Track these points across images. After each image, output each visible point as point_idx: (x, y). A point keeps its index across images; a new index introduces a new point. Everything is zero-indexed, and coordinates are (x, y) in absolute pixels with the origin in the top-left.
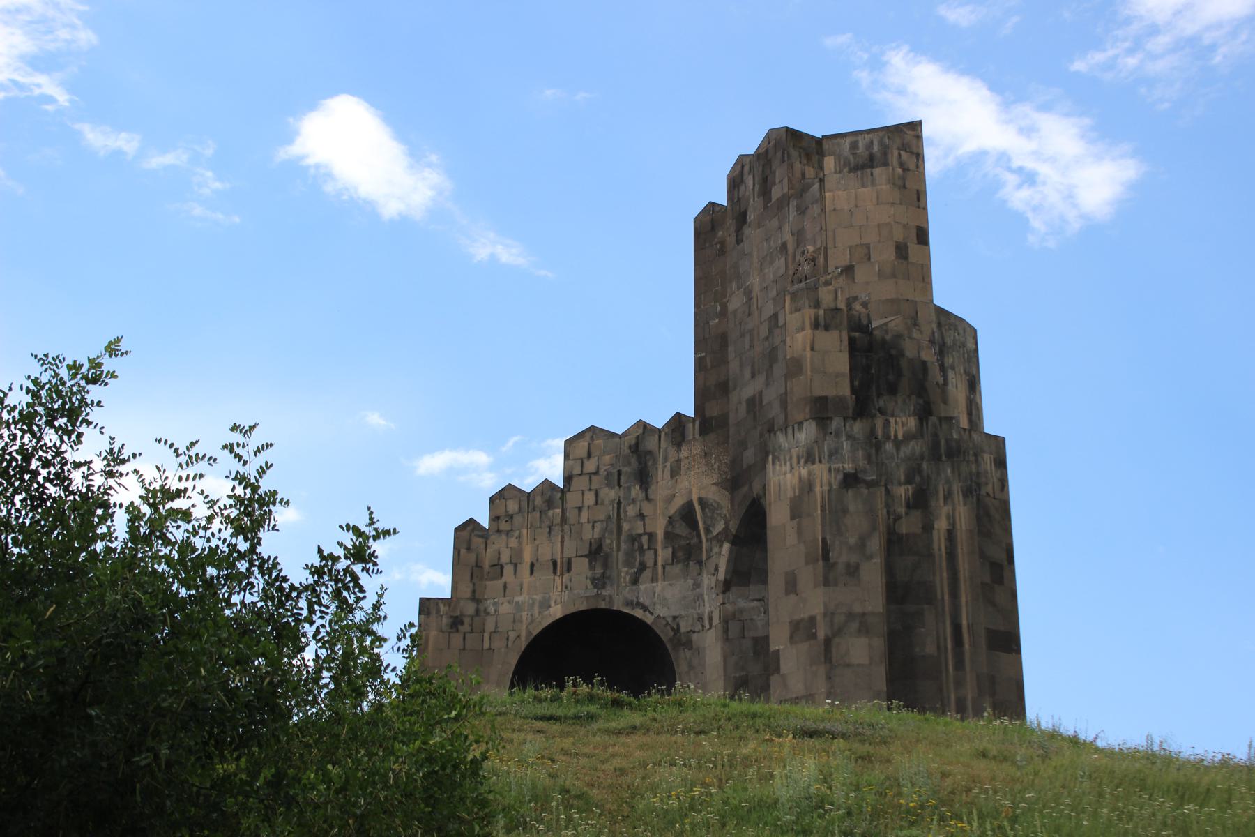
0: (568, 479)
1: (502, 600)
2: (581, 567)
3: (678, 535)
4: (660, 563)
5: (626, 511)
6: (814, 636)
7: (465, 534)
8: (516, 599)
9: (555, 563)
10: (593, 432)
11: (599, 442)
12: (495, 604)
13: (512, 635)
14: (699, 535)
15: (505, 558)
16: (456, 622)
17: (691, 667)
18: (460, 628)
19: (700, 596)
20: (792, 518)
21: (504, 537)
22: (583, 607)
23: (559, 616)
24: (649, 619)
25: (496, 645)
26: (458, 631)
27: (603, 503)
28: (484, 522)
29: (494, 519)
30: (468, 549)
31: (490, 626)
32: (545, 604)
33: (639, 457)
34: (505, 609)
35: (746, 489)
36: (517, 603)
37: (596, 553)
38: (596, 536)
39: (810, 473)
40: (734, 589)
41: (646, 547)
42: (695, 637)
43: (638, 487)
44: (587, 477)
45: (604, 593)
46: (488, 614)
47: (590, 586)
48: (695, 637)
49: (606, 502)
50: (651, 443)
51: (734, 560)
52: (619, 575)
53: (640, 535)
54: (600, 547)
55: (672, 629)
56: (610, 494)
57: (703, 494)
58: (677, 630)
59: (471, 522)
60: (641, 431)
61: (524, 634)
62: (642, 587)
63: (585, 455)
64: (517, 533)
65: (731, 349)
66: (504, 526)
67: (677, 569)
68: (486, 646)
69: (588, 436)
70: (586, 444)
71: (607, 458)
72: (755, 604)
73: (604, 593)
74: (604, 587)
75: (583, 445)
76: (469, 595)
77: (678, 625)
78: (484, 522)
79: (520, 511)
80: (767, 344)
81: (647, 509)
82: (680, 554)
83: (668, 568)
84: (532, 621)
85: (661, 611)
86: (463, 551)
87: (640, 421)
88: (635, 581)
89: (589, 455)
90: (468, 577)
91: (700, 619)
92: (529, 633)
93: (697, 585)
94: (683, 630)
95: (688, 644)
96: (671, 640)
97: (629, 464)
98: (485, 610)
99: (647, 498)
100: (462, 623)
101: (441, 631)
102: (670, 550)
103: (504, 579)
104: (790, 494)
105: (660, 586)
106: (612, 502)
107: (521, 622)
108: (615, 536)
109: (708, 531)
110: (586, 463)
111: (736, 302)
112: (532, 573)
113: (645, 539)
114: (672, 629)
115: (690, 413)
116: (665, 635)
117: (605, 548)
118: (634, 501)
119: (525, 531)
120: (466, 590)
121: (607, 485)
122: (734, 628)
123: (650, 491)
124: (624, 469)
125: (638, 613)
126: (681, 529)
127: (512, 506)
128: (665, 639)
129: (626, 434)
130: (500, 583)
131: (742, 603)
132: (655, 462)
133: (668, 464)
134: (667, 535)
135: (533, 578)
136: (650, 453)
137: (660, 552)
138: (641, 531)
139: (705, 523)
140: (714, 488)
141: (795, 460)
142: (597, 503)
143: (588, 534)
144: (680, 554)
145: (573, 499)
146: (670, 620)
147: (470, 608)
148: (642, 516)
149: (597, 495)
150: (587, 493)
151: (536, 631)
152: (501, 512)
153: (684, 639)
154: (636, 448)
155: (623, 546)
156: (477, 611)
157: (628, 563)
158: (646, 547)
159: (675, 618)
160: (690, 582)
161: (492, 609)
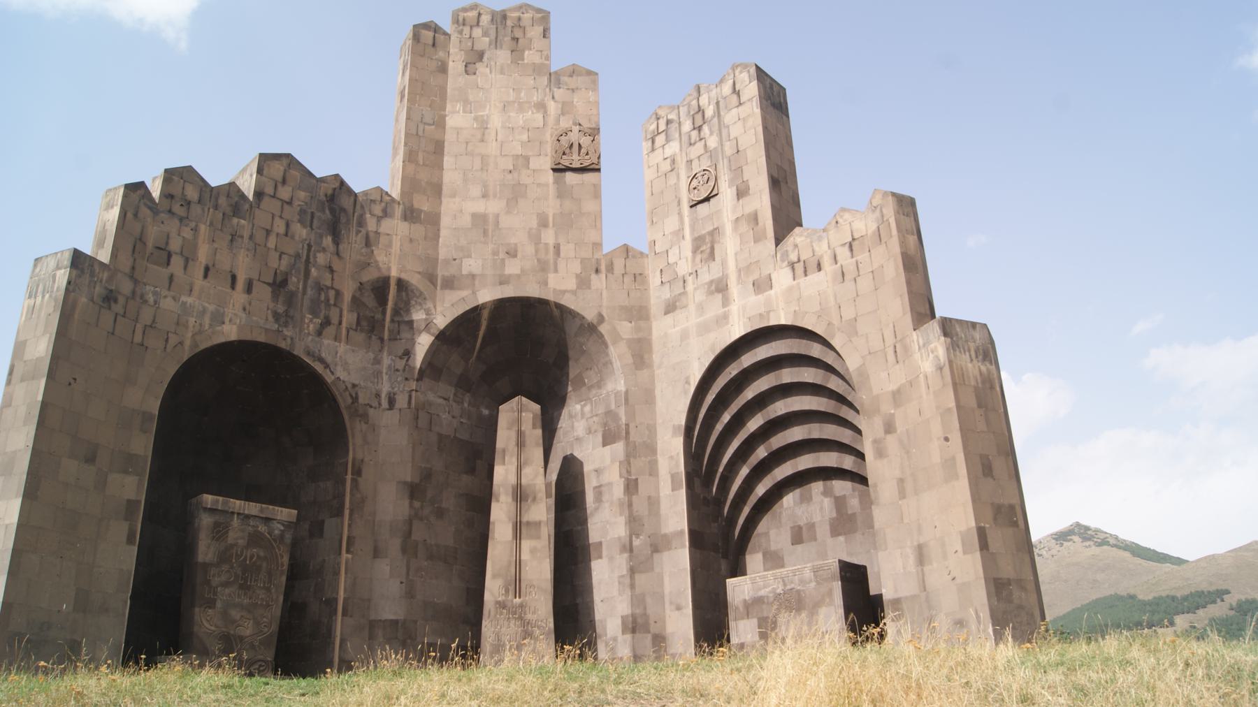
0: (259, 194)
1: (164, 292)
2: (263, 292)
3: (364, 304)
4: (344, 324)
5: (315, 257)
6: (1015, 524)
7: (135, 197)
8: (183, 298)
9: (234, 278)
10: (289, 160)
11: (295, 173)
12: (155, 293)
13: (173, 340)
14: (384, 313)
15: (175, 245)
16: (110, 298)
18: (113, 305)
19: (378, 374)
20: (980, 406)
21: (177, 222)
22: (261, 338)
23: (233, 337)
24: (329, 378)
26: (110, 308)
27: (293, 237)
28: (156, 190)
29: (167, 195)
30: (136, 215)
31: (146, 316)
32: (218, 319)
33: (332, 211)
34: (167, 304)
35: (464, 293)
36: (184, 304)
37: (279, 284)
38: (283, 268)
39: (988, 370)
40: (426, 380)
41: (332, 302)
43: (330, 239)
44: (279, 203)
45: (288, 332)
46: (146, 302)
47: (271, 318)
48: (371, 411)
49: (297, 238)
50: (346, 202)
51: (432, 352)
52: (303, 318)
53: (328, 288)
54: (284, 282)
56: (301, 232)
57: (404, 276)
58: (355, 399)
59: (141, 185)
60: (337, 185)
61: (188, 343)
62: (326, 342)
63: (280, 179)
64: (193, 225)
65: (448, 161)
66: (177, 208)
67: (359, 337)
68: (138, 339)
69: (285, 162)
70: (282, 168)
71: (302, 195)
72: (441, 401)
73: (286, 332)
74: (286, 325)
75: (277, 170)
76: (127, 270)
78: (156, 192)
79: (199, 202)
80: (510, 177)
81: (337, 265)
82: (364, 323)
83: (351, 332)
84: (200, 332)
86: (129, 215)
87: (337, 176)
88: (319, 333)
89: (284, 182)
90: (131, 247)
91: (378, 395)
92: (195, 344)
93: (377, 361)
94: (361, 401)
95: (365, 417)
97: (323, 211)
98: (142, 296)
99: (338, 254)
100: (116, 301)
101: (92, 300)
102: (355, 315)
103: (171, 269)
104: (973, 383)
105: (342, 348)
106: (303, 241)
107: (186, 327)
108: (302, 276)
109: (396, 312)
110: (280, 187)
111: (457, 119)
112: (206, 276)
113: (332, 293)
115: (395, 193)
116: (344, 401)
117: (291, 287)
118: (324, 250)
119: (203, 228)
120: (125, 263)
121: (299, 221)
122: (423, 421)
123: (341, 247)
124: (318, 214)
125: (319, 367)
126: (370, 300)
127: (192, 193)
128: (342, 405)
129: (322, 180)
130: (165, 272)
131: (431, 397)
132: (348, 222)
133: (364, 231)
134: (356, 302)
135: (205, 283)
136: (343, 210)
137: (345, 313)
138: (328, 283)
139: (396, 304)
140: (418, 276)
141: (973, 353)
142: (286, 235)
143: (274, 264)
144: (364, 323)
145: (262, 218)
146: (349, 386)
147: (126, 287)
148: (331, 270)
149: (288, 225)
150: (277, 220)
152: (176, 191)
154: (332, 198)
155: (309, 292)
156: (134, 292)
157: (315, 313)
158: (332, 302)
159: (354, 386)
160: (371, 355)
161: (151, 299)
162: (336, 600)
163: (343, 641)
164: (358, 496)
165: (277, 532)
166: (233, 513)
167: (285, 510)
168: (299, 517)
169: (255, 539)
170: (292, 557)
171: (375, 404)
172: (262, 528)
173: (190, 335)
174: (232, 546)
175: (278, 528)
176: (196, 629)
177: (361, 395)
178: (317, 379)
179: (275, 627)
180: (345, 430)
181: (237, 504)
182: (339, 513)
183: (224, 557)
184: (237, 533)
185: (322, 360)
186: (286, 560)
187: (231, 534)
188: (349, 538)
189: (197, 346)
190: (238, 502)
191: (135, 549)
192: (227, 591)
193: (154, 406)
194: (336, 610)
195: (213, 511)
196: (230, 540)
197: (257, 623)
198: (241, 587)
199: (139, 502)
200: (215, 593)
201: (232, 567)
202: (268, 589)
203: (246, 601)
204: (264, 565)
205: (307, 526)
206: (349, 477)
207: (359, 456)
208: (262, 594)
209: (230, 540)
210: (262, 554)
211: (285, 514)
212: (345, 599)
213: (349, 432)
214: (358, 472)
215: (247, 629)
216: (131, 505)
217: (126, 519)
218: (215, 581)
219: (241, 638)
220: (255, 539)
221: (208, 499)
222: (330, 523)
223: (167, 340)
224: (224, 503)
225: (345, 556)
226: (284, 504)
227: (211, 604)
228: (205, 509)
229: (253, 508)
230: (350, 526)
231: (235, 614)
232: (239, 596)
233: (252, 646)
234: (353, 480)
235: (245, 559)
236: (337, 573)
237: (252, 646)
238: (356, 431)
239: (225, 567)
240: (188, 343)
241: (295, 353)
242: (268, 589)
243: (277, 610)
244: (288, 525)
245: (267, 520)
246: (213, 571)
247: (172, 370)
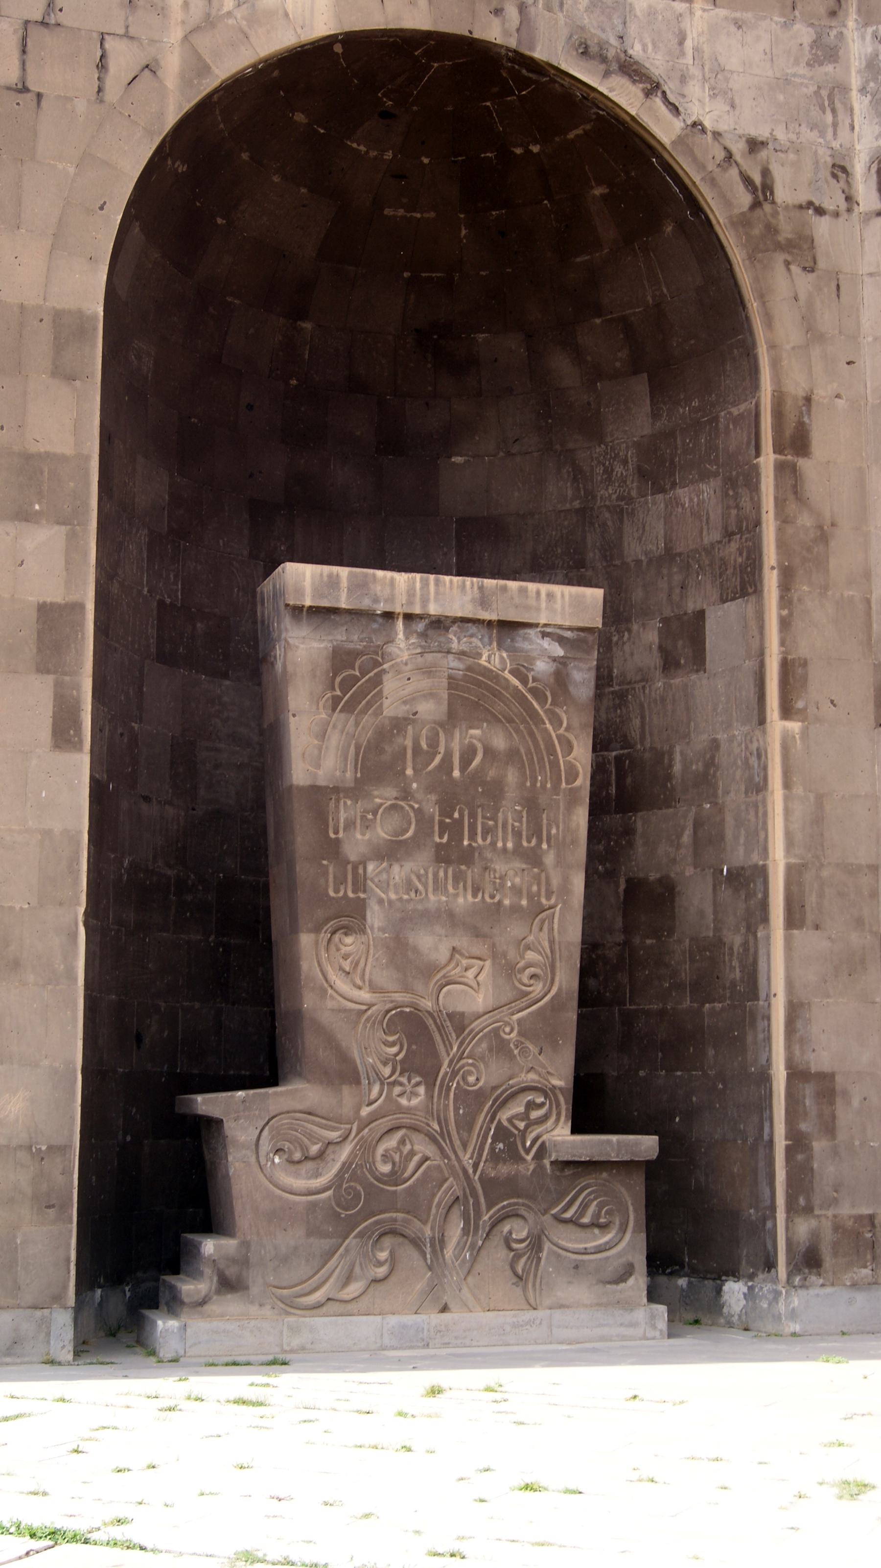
13: (123, 59)
17: (813, 334)
19: (833, 97)
24: (664, 128)
25: (47, 77)
42: (822, 227)
48: (822, 227)
55: (747, 181)
58: (762, 191)
61: (172, 64)
77: (766, 173)
84: (209, 22)
85: (702, 106)
91: (840, 170)
92: (198, 65)
93: (827, 52)
94: (782, 194)
95: (801, 250)
96: (742, 222)
114: (747, 181)
116: (723, 203)
125: (624, 96)
146: (738, 149)
151: (230, 63)
153: (786, 231)
159: (754, 145)
160: (804, 34)
162: (762, 873)
163: (794, 1011)
164: (805, 520)
165: (542, 667)
166: (389, 616)
167: (564, 592)
168: (616, 613)
169: (473, 695)
170: (599, 745)
171: (833, 200)
172: (492, 657)
173: (176, 34)
174: (399, 725)
175: (543, 654)
176: (309, 1001)
177: (781, 176)
178: (624, 141)
179: (567, 978)
180: (741, 302)
181: (398, 587)
182: (747, 583)
183: (377, 762)
184: (409, 683)
185: (631, 70)
186: (581, 756)
187: (390, 685)
188: (786, 666)
189: (204, 69)
190: (401, 579)
191: (79, 766)
192: (398, 872)
193: (86, 288)
194: (764, 906)
195: (322, 614)
196: (391, 707)
197: (508, 970)
198: (443, 856)
199: (78, 607)
200: (360, 884)
201: (406, 794)
202: (534, 858)
203: (464, 901)
204: (512, 777)
205: (651, 636)
206: (768, 460)
207: (796, 384)
208: (512, 873)
209: (391, 707)
210: (500, 742)
211: (567, 605)
212: (793, 874)
213: (754, 306)
214: (796, 442)
215: (475, 993)
216: (52, 619)
217: (42, 669)
218: (356, 844)
219: (460, 1022)
220: (473, 695)
221: (301, 579)
222: (722, 621)
223: (102, 65)
224: (358, 587)
225: (777, 726)
226: (576, 575)
227: (350, 917)
228: (297, 611)
229: (452, 594)
230: (785, 624)
231: (432, 944)
232: (438, 887)
233: (500, 1047)
234: (781, 468)
235: (446, 765)
236: (759, 786)
237: (500, 1047)
238: (776, 303)
239: (384, 795)
240: (172, 64)
241: (539, 54)
242: (534, 858)
243: (569, 927)
244: (576, 640)
245: (507, 628)
246: (345, 811)
247: (132, 159)
